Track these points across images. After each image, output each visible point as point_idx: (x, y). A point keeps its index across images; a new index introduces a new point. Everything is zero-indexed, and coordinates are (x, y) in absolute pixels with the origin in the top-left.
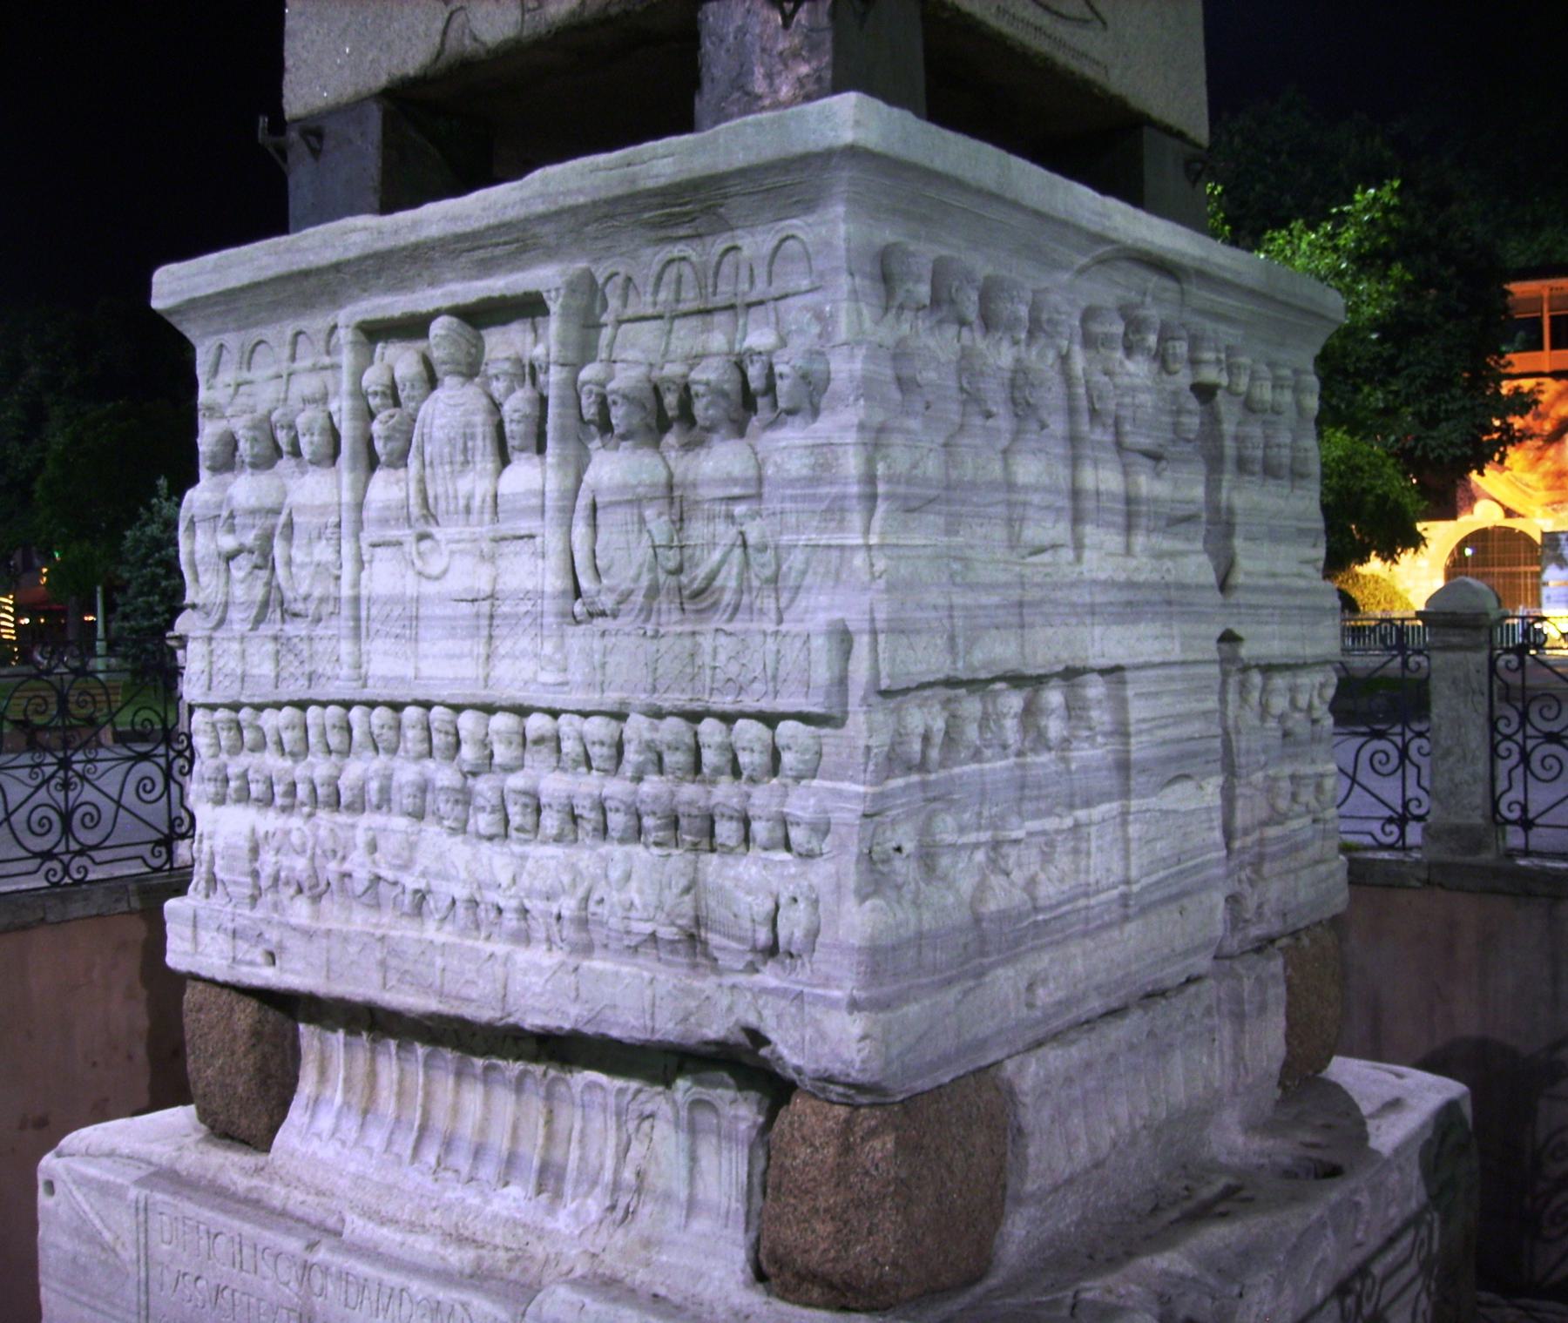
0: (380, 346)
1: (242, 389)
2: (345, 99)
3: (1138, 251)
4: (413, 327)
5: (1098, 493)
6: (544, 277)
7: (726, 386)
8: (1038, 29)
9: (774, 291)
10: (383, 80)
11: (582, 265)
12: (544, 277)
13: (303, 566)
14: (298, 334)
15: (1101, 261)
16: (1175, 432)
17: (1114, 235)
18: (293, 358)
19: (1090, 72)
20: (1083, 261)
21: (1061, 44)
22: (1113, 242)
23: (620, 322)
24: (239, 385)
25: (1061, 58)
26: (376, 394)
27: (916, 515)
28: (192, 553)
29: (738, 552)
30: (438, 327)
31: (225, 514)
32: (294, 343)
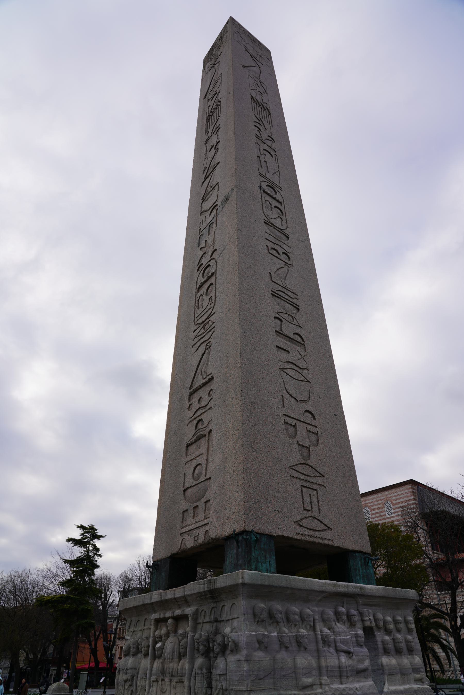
0: (160, 624)
1: (134, 633)
2: (163, 558)
3: (336, 593)
4: (165, 620)
5: (327, 667)
6: (189, 611)
7: (220, 643)
8: (309, 536)
9: (231, 618)
11: (197, 607)
12: (189, 611)
13: (139, 686)
14: (146, 619)
15: (325, 597)
16: (357, 643)
17: (326, 591)
18: (144, 625)
19: (327, 542)
20: (319, 598)
21: (317, 538)
22: (327, 592)
23: (203, 623)
24: (134, 632)
25: (317, 541)
26: (157, 637)
27: (262, 680)
28: (118, 679)
29: (221, 690)
30: (170, 621)
31: (126, 668)
32: (145, 621)
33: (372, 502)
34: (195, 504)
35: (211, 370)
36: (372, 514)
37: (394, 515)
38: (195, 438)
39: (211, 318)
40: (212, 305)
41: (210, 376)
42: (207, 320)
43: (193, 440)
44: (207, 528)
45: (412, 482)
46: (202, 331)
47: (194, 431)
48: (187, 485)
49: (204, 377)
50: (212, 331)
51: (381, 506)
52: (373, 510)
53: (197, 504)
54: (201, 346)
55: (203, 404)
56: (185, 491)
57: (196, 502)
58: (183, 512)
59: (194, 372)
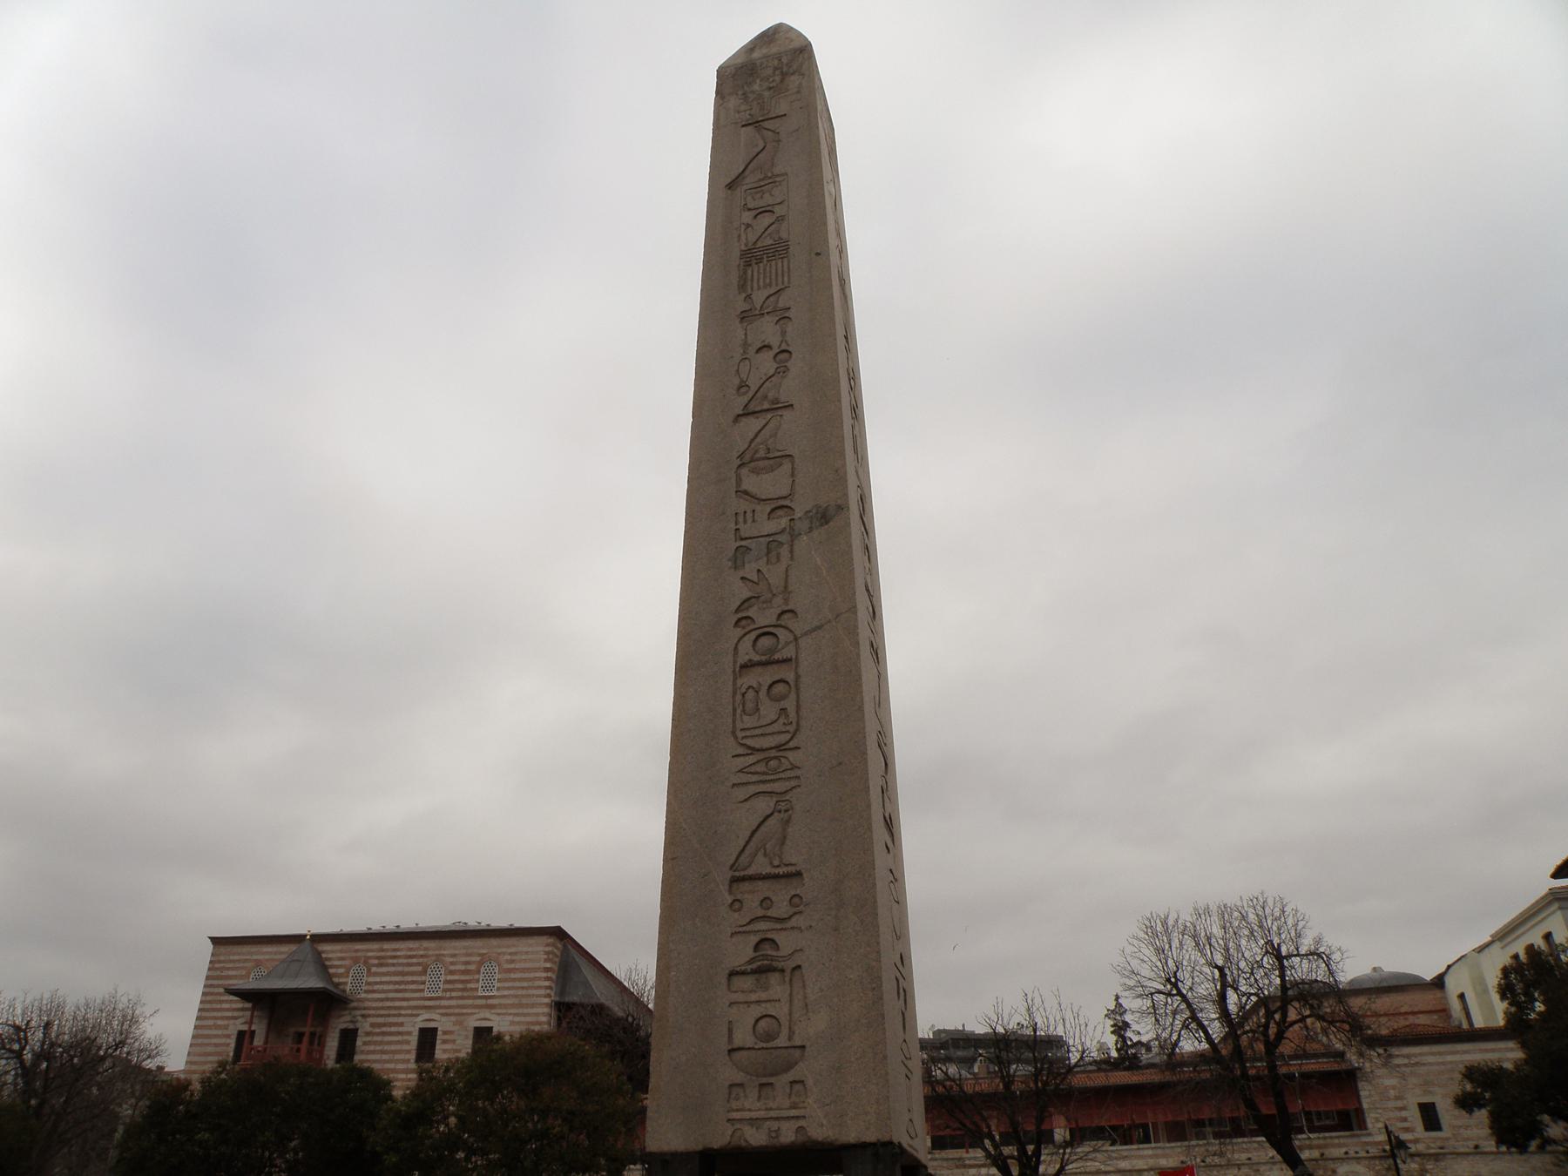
10: (700, 1148)
33: (454, 956)
34: (764, 1080)
35: (795, 856)
36: (447, 982)
37: (495, 993)
38: (754, 966)
39: (790, 754)
40: (792, 728)
41: (791, 869)
42: (773, 753)
43: (749, 968)
44: (802, 1123)
45: (558, 933)
46: (760, 768)
47: (750, 953)
48: (737, 1043)
49: (776, 863)
50: (793, 783)
51: (472, 967)
52: (452, 973)
53: (771, 1080)
54: (761, 798)
55: (771, 913)
56: (730, 1051)
57: (772, 1075)
58: (731, 1086)
59: (742, 843)
